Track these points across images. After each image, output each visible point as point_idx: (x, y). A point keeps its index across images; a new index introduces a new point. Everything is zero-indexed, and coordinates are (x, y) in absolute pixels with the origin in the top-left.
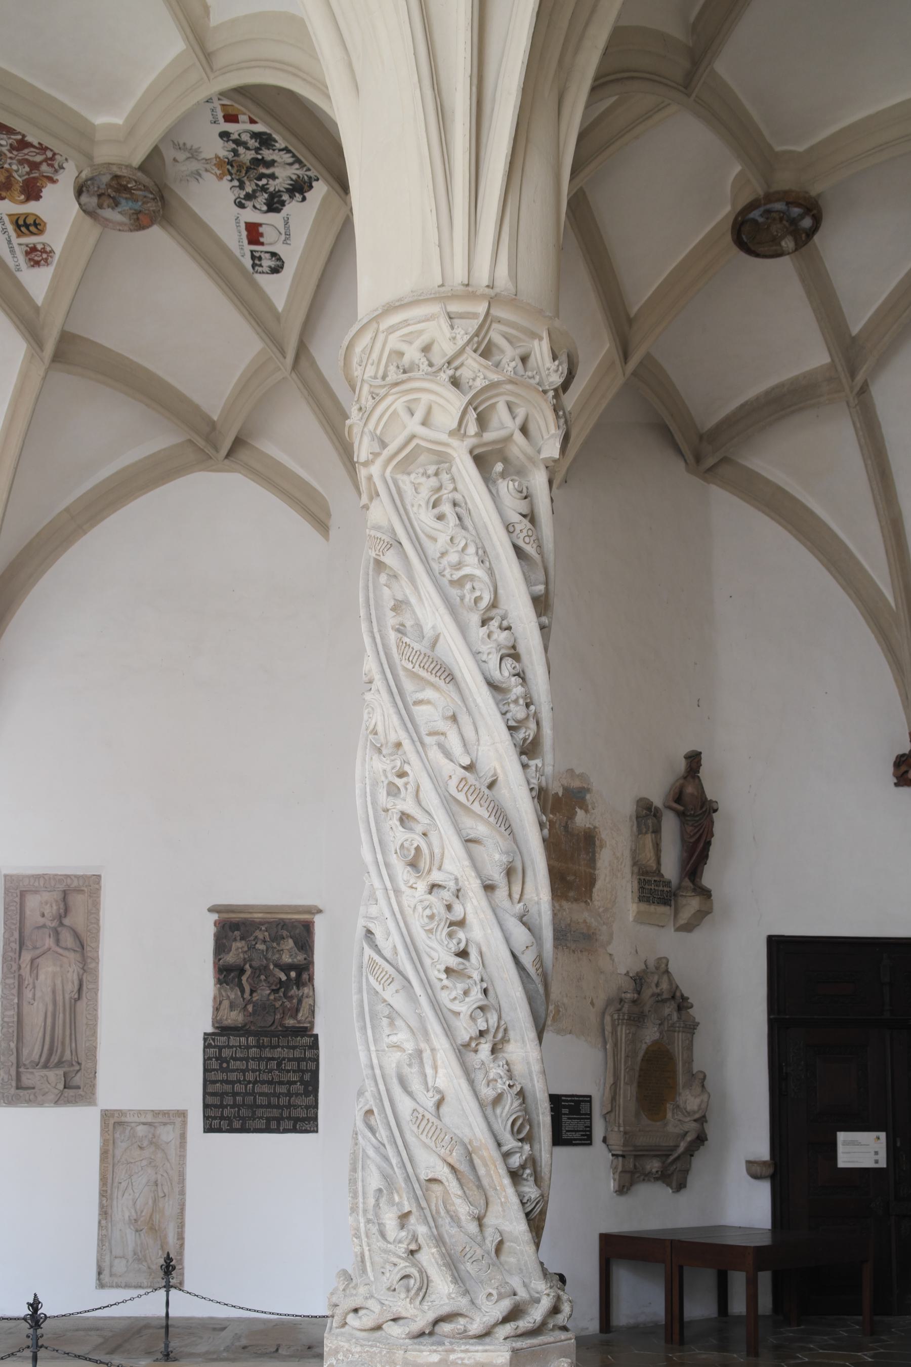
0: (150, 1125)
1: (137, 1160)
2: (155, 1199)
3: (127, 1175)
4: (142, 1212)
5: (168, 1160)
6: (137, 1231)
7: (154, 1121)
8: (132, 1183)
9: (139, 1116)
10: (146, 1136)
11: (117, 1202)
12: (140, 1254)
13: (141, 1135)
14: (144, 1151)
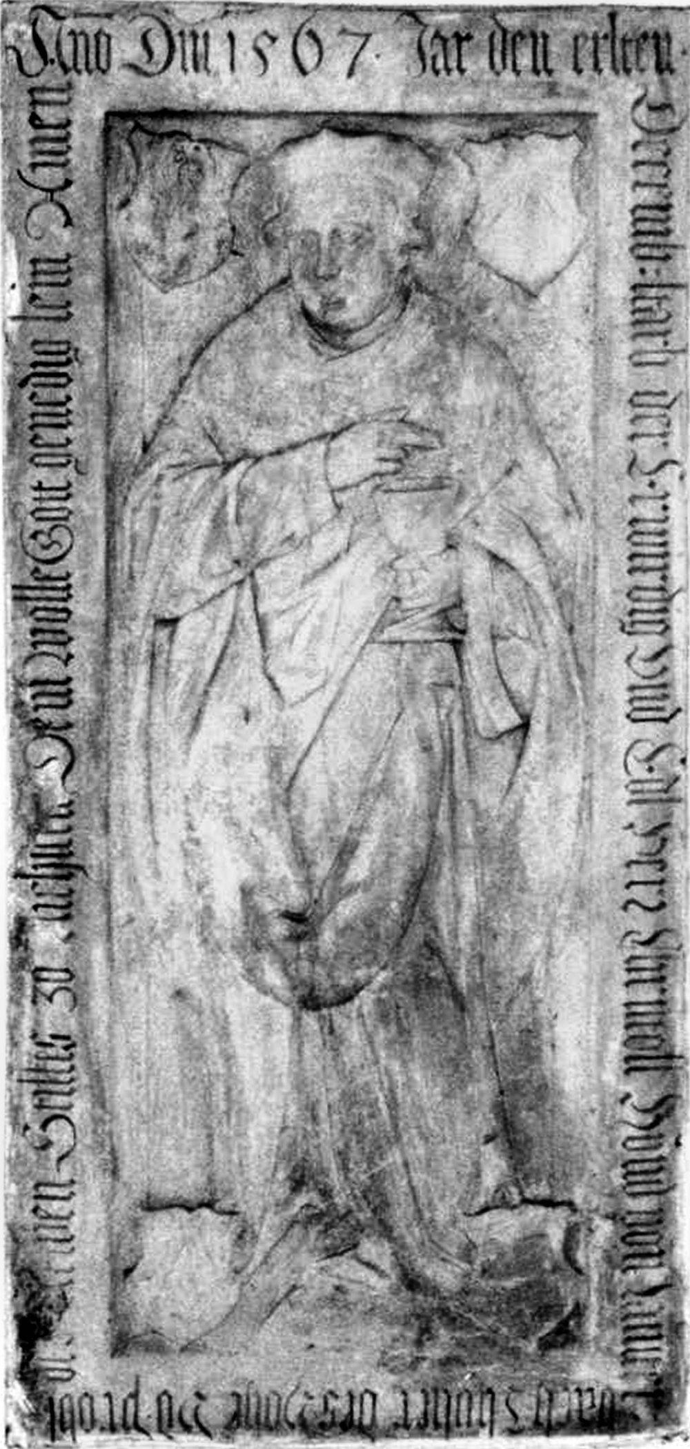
0: (395, 138)
1: (295, 433)
2: (449, 756)
3: (218, 562)
4: (346, 852)
5: (538, 434)
6: (310, 1001)
7: (423, 102)
8: (262, 624)
9: (308, 54)
10: (363, 238)
11: (149, 771)
12: (335, 1178)
13: (324, 228)
14: (354, 360)
